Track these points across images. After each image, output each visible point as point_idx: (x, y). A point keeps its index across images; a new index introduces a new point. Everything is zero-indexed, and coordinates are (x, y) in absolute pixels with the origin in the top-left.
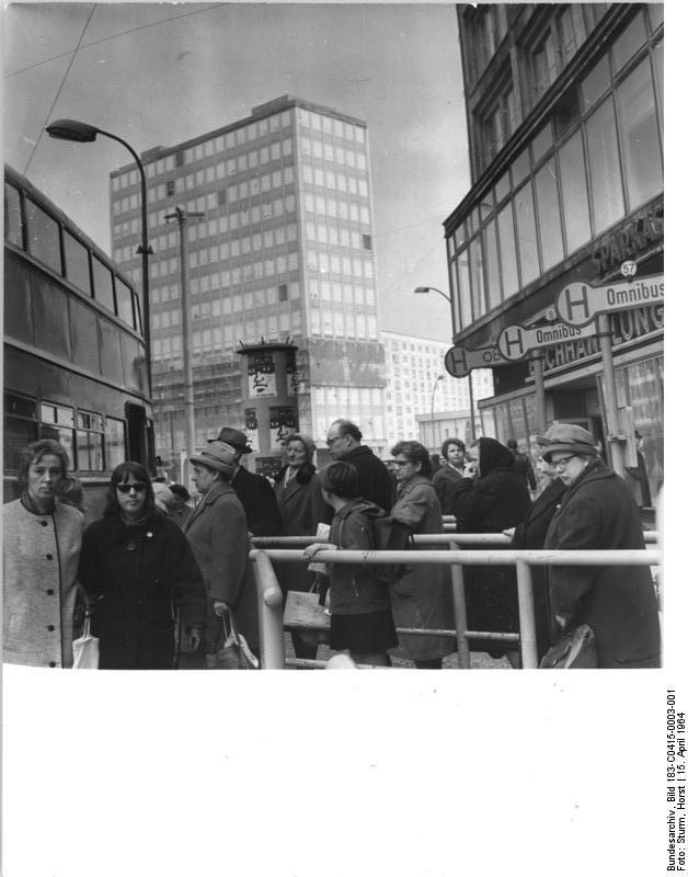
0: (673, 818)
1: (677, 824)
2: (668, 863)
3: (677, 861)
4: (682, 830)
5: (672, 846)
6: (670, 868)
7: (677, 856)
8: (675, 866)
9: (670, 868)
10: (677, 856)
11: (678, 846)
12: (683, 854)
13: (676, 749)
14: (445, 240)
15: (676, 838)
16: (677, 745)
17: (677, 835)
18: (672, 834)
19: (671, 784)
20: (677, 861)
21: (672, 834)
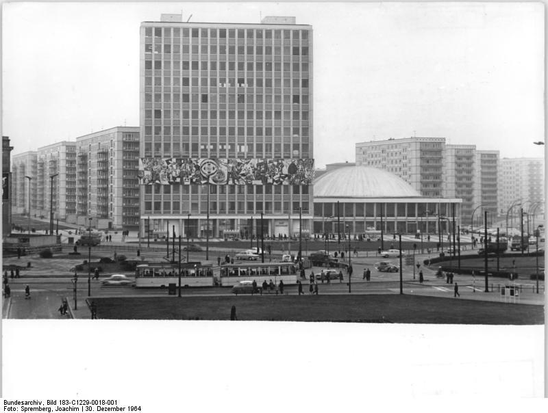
0: (37, 404)
2: (9, 401)
3: (10, 406)
5: (19, 403)
6: (5, 402)
7: (13, 406)
8: (7, 405)
9: (5, 402)
10: (13, 406)
11: (19, 407)
12: (14, 409)
15: (24, 405)
17: (27, 406)
18: (27, 403)
19: (58, 403)
20: (10, 406)
21: (27, 403)
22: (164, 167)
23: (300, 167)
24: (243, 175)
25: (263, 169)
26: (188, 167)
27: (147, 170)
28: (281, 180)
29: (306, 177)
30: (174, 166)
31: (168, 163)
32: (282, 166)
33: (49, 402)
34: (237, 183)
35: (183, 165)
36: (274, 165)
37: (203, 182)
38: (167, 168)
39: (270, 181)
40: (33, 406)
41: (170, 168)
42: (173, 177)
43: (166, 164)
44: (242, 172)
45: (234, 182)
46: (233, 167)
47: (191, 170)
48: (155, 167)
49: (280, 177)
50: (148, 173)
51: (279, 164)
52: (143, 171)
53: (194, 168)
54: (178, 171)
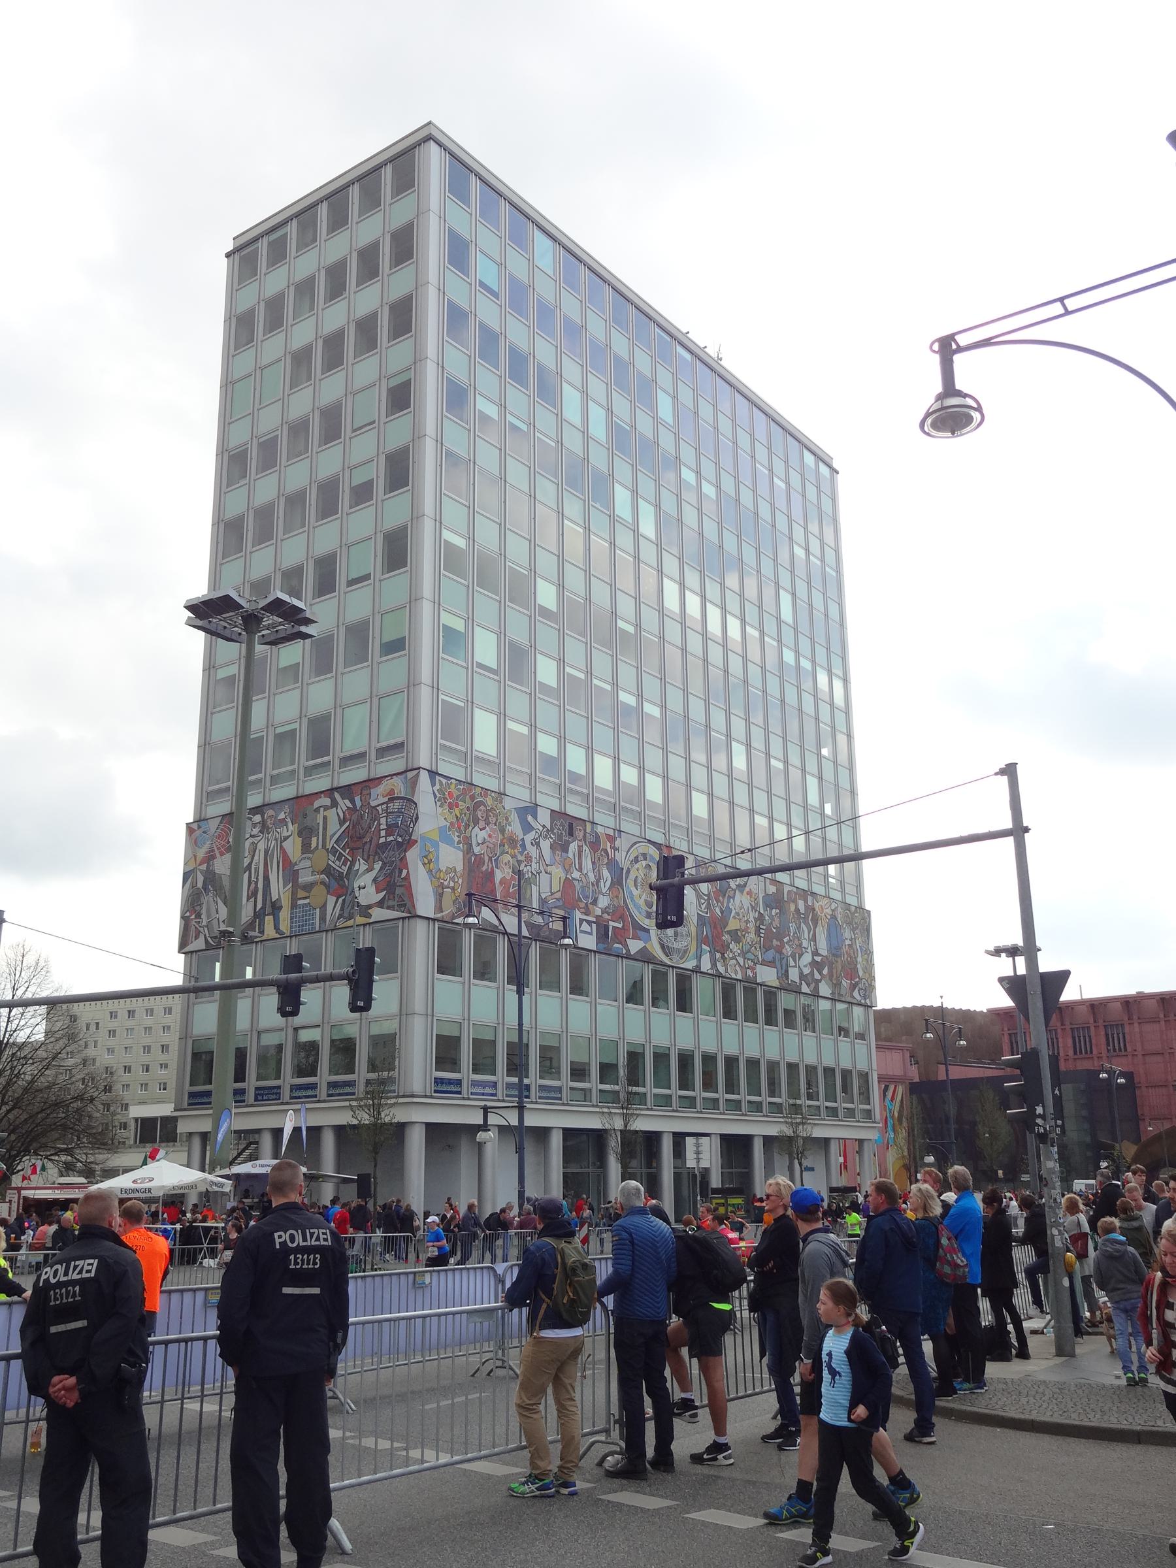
22: (513, 842)
23: (847, 934)
24: (736, 936)
25: (776, 922)
26: (587, 863)
27: (449, 842)
28: (817, 976)
29: (861, 973)
30: (545, 845)
31: (528, 828)
32: (815, 921)
34: (722, 970)
35: (573, 847)
36: (797, 910)
37: (634, 946)
38: (523, 846)
39: (794, 975)
41: (532, 851)
42: (543, 901)
43: (515, 828)
44: (733, 925)
45: (714, 965)
46: (708, 895)
47: (598, 882)
48: (479, 835)
49: (814, 964)
50: (451, 858)
51: (807, 907)
52: (437, 846)
53: (606, 874)
54: (558, 872)
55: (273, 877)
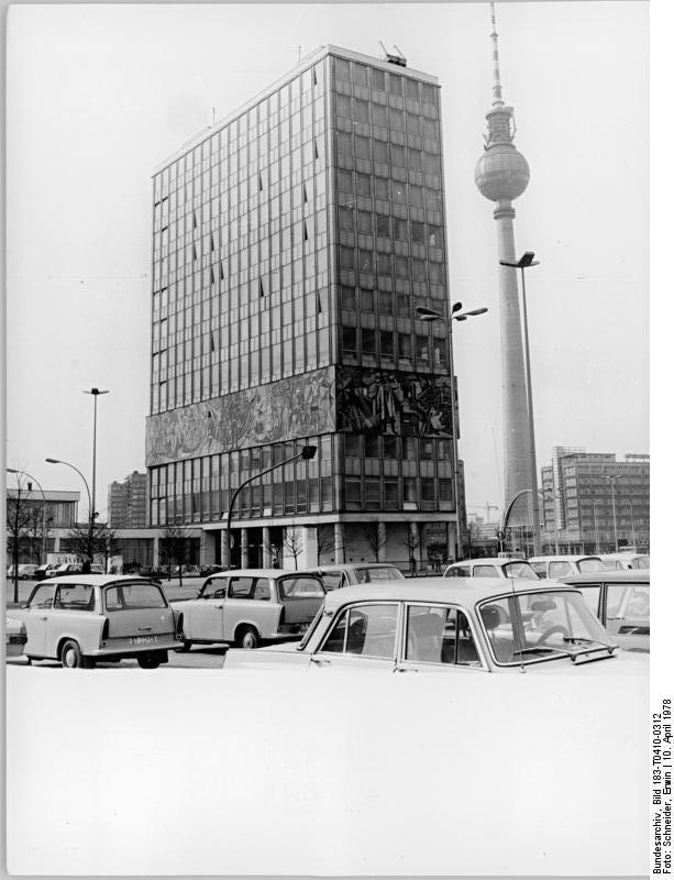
1: (663, 828)
3: (663, 864)
4: (668, 830)
5: (658, 849)
6: (657, 871)
7: (663, 859)
8: (661, 869)
10: (663, 859)
12: (668, 857)
13: (662, 736)
14: (496, 224)
15: (662, 842)
16: (663, 730)
17: (663, 837)
18: (658, 837)
20: (663, 864)
21: (658, 837)
33: (657, 802)
40: (663, 824)
55: (389, 405)
